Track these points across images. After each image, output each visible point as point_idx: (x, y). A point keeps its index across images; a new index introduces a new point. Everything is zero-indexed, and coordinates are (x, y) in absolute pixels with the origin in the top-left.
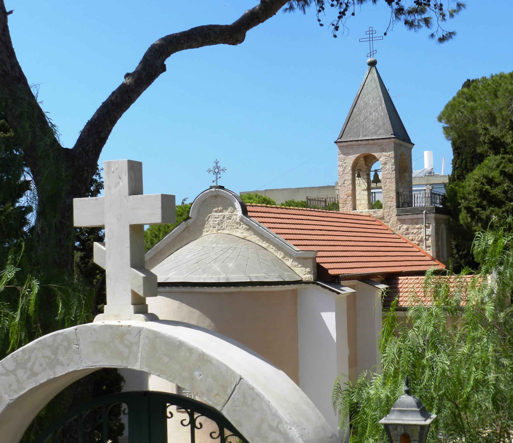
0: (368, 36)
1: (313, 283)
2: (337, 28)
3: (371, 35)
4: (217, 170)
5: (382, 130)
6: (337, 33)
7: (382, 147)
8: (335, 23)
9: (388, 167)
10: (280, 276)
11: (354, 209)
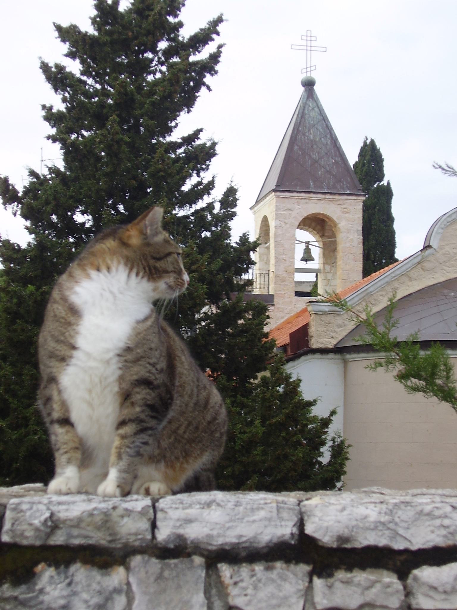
3: (309, 42)
9: (351, 237)
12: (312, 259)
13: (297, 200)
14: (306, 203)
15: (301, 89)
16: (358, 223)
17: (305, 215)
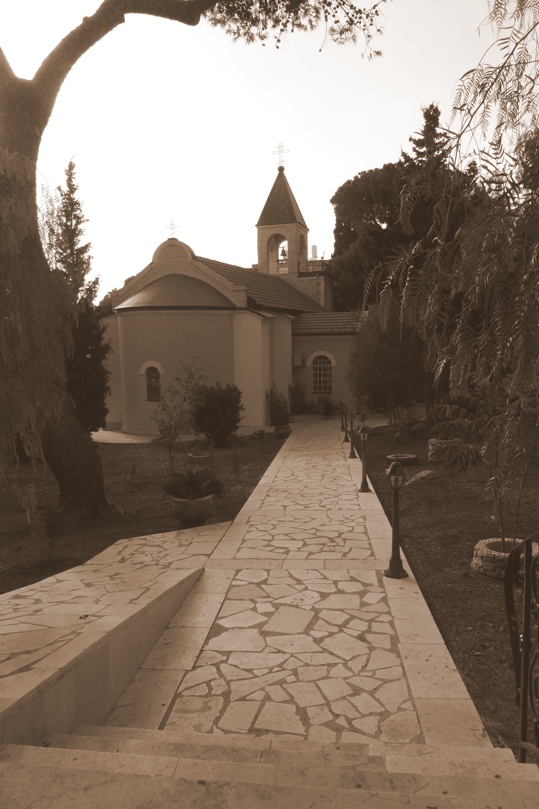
0: (278, 150)
2: (279, 41)
4: (172, 226)
6: (278, 44)
8: (277, 36)
12: (286, 255)
15: (278, 172)
17: (271, 235)
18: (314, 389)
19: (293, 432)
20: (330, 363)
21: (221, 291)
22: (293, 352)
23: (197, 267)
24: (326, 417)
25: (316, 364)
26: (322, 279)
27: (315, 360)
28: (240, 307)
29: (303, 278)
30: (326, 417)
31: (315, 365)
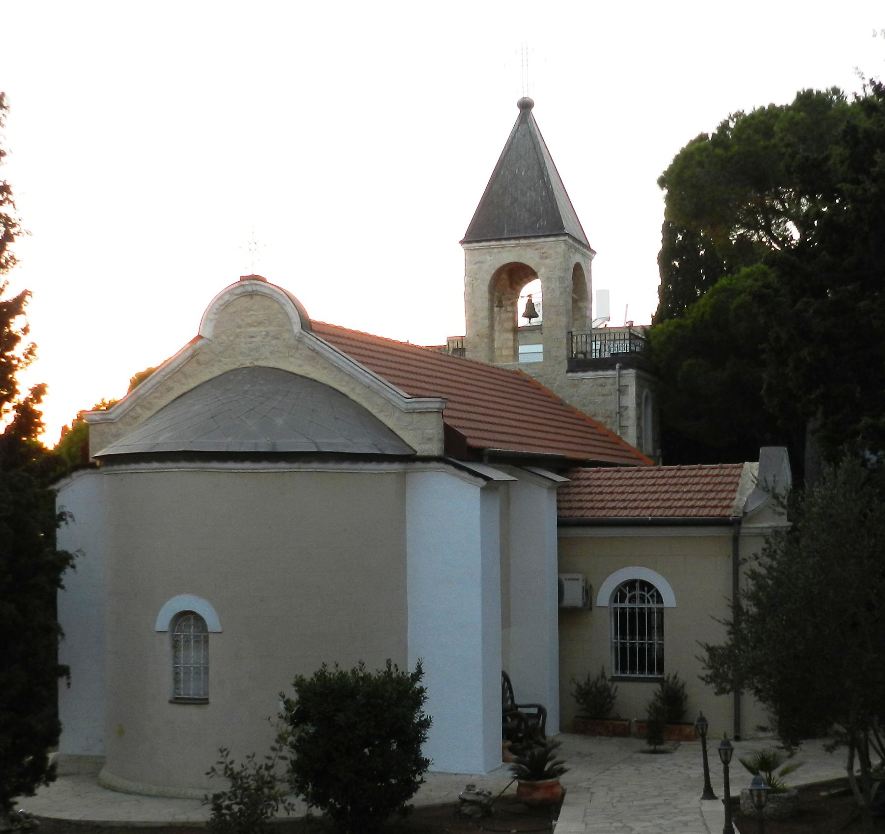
1: (438, 459)
5: (543, 222)
7: (543, 251)
9: (553, 286)
10: (376, 446)
11: (491, 360)
13: (489, 250)
14: (499, 252)
16: (560, 269)
17: (498, 266)
18: (617, 668)
19: (567, 798)
20: (660, 599)
21: (374, 411)
22: (561, 570)
23: (314, 350)
24: (652, 747)
25: (622, 601)
26: (630, 376)
27: (620, 590)
28: (426, 454)
29: (580, 375)
30: (652, 747)
31: (619, 605)
